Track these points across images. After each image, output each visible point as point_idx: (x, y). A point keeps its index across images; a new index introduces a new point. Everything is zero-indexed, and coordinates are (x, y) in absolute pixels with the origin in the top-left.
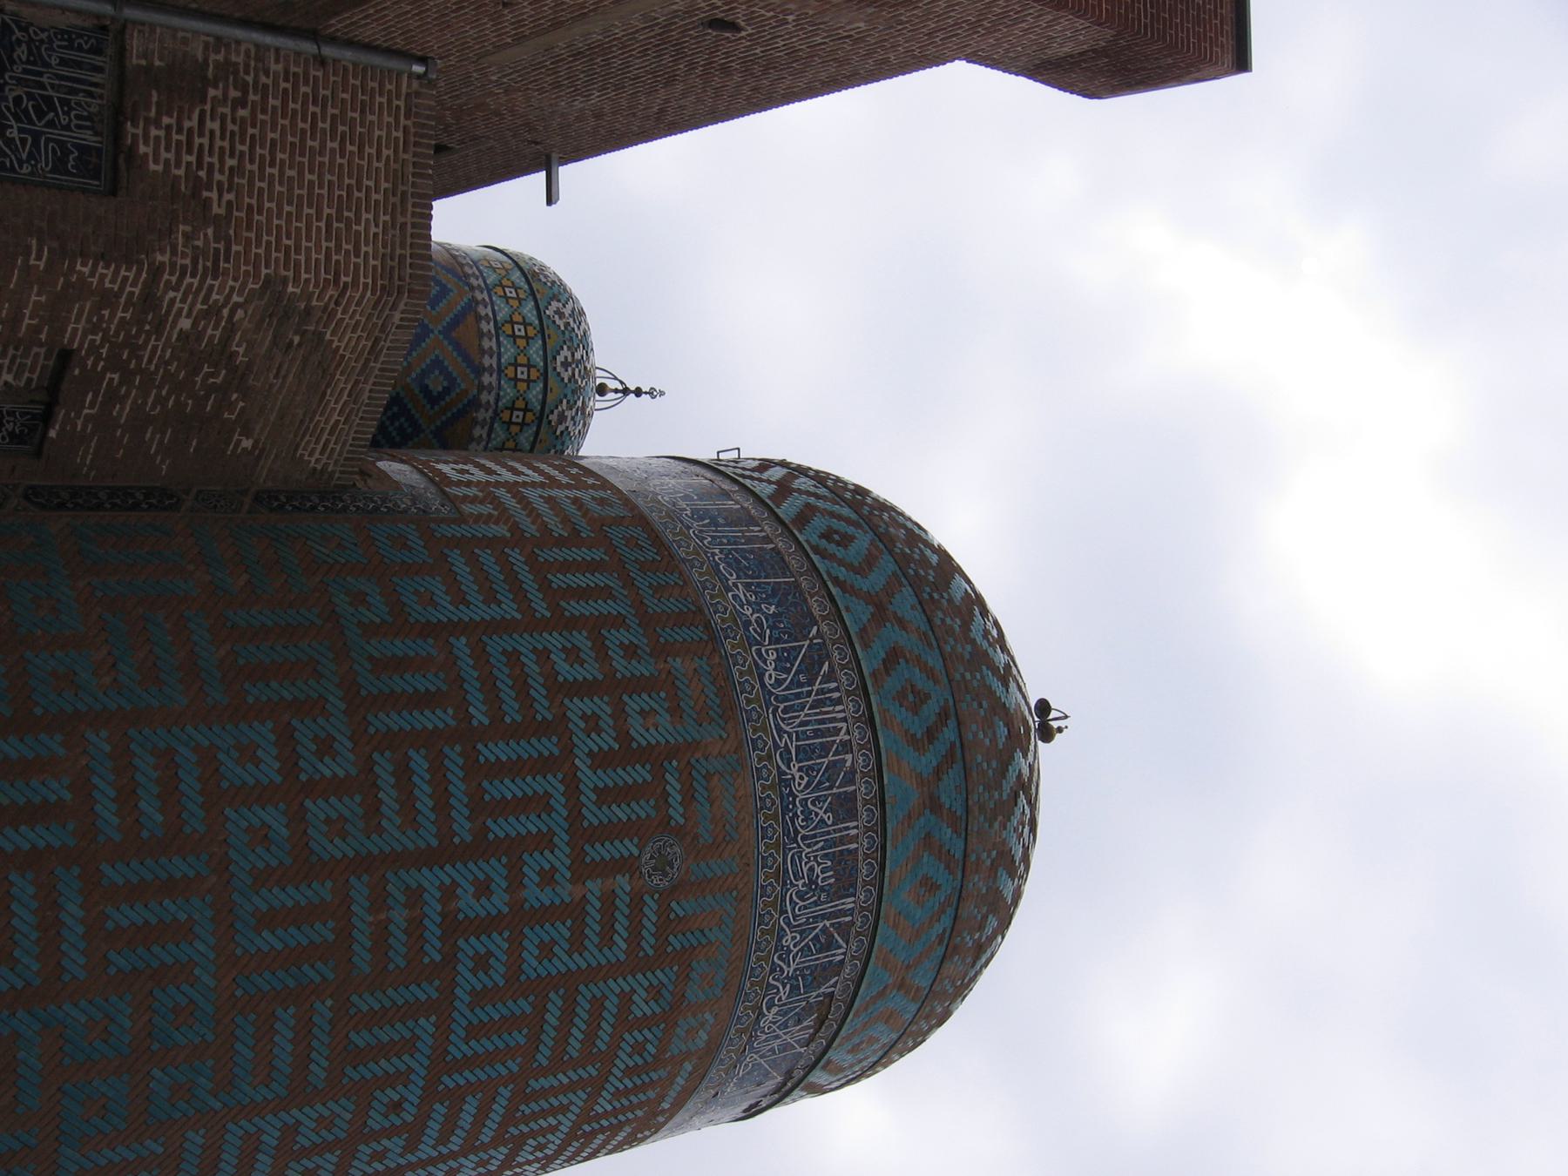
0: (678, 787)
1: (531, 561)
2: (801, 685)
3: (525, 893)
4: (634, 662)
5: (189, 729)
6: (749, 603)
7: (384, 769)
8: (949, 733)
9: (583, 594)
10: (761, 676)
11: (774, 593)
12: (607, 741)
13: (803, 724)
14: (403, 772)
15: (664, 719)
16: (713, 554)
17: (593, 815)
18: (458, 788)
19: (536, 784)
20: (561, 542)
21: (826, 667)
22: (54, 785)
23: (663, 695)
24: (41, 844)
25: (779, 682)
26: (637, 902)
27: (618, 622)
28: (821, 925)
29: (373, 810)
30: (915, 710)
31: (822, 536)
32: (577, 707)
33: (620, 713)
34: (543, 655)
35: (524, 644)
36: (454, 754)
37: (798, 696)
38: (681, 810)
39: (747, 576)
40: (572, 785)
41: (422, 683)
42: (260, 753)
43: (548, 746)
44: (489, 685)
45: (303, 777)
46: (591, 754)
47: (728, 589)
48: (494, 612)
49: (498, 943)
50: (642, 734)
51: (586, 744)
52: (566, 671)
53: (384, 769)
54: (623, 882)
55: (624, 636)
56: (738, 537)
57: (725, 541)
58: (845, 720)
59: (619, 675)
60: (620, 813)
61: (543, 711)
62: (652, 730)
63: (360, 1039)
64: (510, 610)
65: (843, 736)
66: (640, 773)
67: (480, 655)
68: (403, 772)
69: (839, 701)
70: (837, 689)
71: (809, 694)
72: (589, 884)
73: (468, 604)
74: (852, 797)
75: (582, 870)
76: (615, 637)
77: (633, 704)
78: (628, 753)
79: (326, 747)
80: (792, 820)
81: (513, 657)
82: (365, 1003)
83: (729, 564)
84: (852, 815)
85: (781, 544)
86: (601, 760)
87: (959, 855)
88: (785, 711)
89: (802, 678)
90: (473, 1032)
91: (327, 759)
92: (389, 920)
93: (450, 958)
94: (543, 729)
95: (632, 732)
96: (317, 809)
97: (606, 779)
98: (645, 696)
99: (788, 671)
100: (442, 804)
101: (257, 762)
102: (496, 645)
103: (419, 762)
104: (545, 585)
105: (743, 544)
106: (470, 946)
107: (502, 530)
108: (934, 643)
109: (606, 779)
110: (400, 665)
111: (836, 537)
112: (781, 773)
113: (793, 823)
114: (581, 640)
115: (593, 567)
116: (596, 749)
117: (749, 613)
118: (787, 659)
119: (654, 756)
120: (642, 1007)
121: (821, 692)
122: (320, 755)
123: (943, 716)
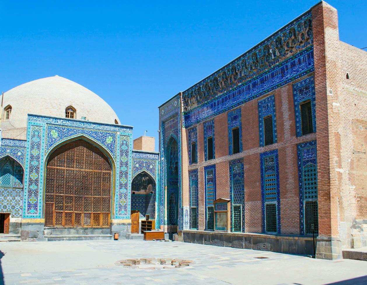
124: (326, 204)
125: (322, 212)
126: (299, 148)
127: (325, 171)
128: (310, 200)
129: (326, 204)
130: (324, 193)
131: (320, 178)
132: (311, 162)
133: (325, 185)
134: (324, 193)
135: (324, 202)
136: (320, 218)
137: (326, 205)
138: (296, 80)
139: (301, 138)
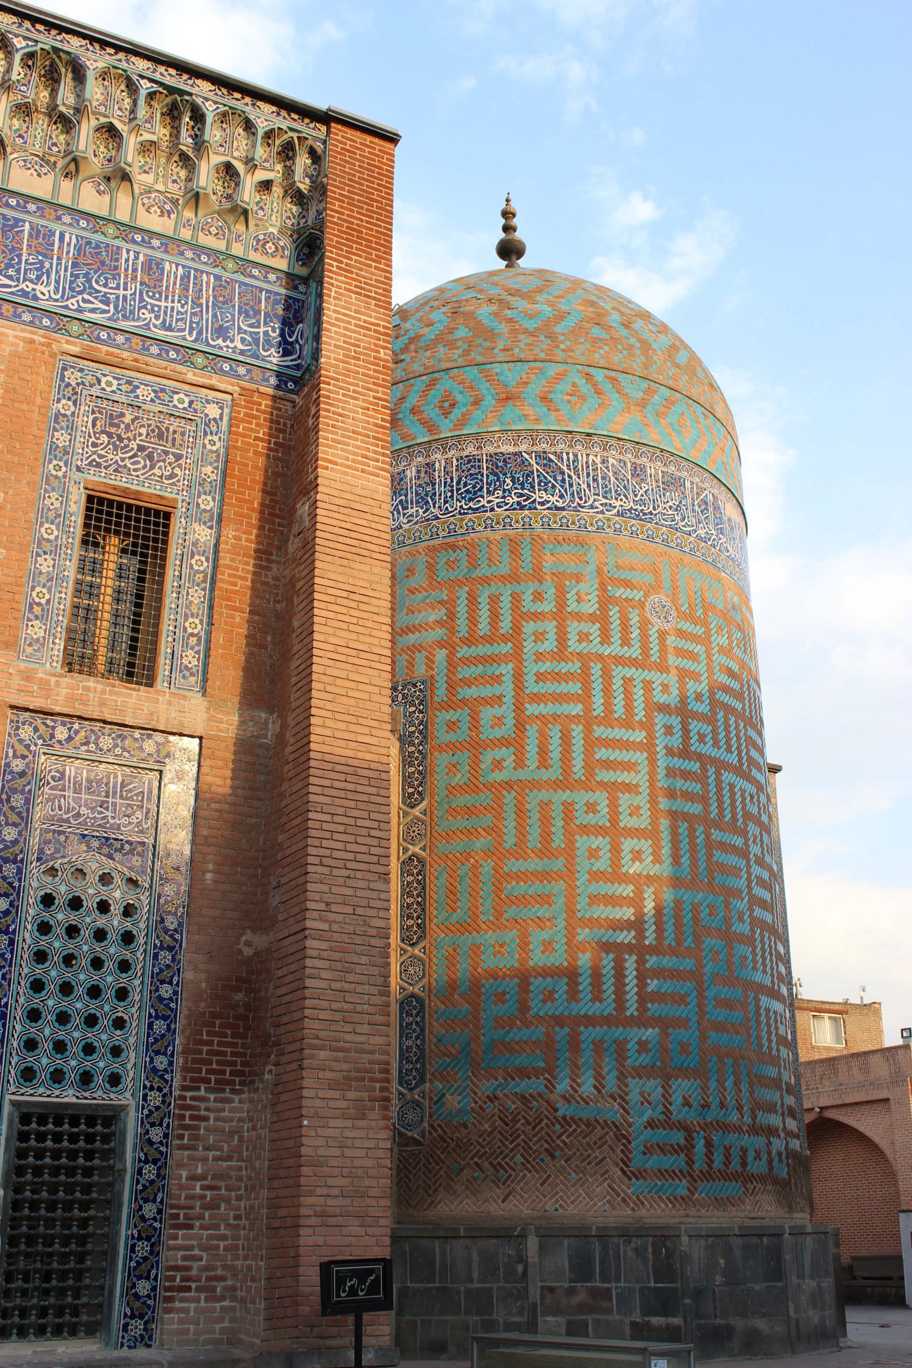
0: (622, 590)
1: (470, 641)
2: (563, 481)
3: (673, 705)
4: (545, 596)
5: (578, 883)
6: (504, 497)
7: (604, 776)
8: (599, 375)
9: (495, 615)
10: (557, 508)
11: (496, 475)
12: (594, 629)
13: (589, 486)
14: (608, 765)
15: (583, 587)
16: (461, 507)
17: (635, 652)
18: (619, 733)
19: (617, 684)
20: (452, 615)
21: (553, 457)
22: (605, 962)
23: (567, 583)
24: (635, 973)
25: (561, 496)
26: (680, 633)
27: (516, 599)
28: (696, 508)
29: (629, 788)
30: (583, 398)
31: (446, 414)
32: (573, 644)
33: (578, 616)
34: (539, 657)
35: (531, 668)
36: (599, 731)
37: (571, 485)
38: (635, 591)
39: (481, 489)
40: (620, 661)
41: (555, 742)
42: (594, 847)
43: (596, 670)
44: (559, 698)
45: (608, 824)
46: (602, 643)
47: (492, 510)
48: (508, 679)
49: (695, 726)
50: (590, 607)
51: (595, 646)
52: (550, 645)
53: (604, 776)
54: (671, 641)
55: (527, 598)
56: (445, 483)
57: (449, 494)
58: (588, 455)
59: (555, 610)
60: (635, 633)
61: (574, 667)
62: (590, 597)
63: (728, 817)
64: (506, 670)
65: (598, 460)
66: (614, 612)
67: (537, 698)
68: (608, 765)
69: (576, 456)
70: (568, 454)
71: (570, 476)
72: (670, 663)
73: (502, 696)
74: (635, 467)
75: (663, 668)
76: (528, 603)
77: (572, 606)
78: (601, 618)
79: (591, 808)
80: (645, 514)
81: (540, 677)
82: (714, 808)
83: (471, 500)
84: (643, 469)
85: (452, 452)
86: (605, 638)
87: (668, 392)
88: (581, 499)
89: (559, 478)
90: (729, 750)
91: (599, 808)
92: (681, 790)
93: (700, 757)
94: (586, 672)
95: (590, 611)
96: (626, 821)
97: (616, 637)
98: (568, 596)
99: (554, 487)
100: (626, 745)
101: (598, 849)
102: (532, 687)
103: (602, 754)
104: (487, 640)
105: (452, 479)
106: (695, 746)
107: (441, 655)
108: (539, 364)
109: (616, 637)
110: (543, 752)
111: (446, 404)
112: (618, 514)
113: (645, 514)
114: (529, 628)
115: (473, 600)
116: (599, 639)
117: (511, 501)
118: (546, 484)
119: (605, 602)
120: (724, 641)
121: (568, 466)
122: (595, 812)
123: (589, 377)
124: (362, 1134)
125: (330, 1181)
126: (21, 741)
127: (357, 939)
128: (69, 1096)
129: (362, 1134)
130: (346, 1066)
131: (325, 974)
132: (110, 856)
133: (355, 1017)
134: (346, 1066)
135: (348, 1123)
136: (314, 1221)
137: (358, 1143)
138: (98, 350)
139: (58, 684)
